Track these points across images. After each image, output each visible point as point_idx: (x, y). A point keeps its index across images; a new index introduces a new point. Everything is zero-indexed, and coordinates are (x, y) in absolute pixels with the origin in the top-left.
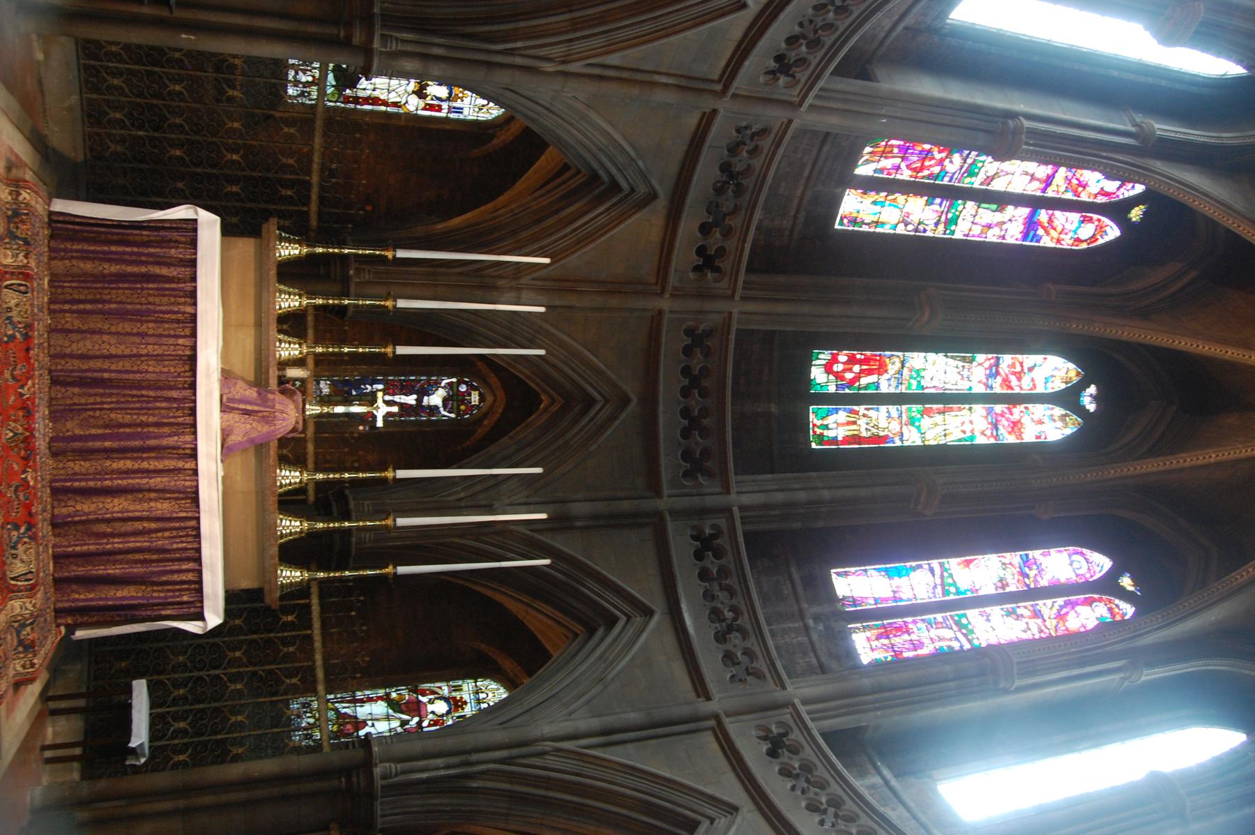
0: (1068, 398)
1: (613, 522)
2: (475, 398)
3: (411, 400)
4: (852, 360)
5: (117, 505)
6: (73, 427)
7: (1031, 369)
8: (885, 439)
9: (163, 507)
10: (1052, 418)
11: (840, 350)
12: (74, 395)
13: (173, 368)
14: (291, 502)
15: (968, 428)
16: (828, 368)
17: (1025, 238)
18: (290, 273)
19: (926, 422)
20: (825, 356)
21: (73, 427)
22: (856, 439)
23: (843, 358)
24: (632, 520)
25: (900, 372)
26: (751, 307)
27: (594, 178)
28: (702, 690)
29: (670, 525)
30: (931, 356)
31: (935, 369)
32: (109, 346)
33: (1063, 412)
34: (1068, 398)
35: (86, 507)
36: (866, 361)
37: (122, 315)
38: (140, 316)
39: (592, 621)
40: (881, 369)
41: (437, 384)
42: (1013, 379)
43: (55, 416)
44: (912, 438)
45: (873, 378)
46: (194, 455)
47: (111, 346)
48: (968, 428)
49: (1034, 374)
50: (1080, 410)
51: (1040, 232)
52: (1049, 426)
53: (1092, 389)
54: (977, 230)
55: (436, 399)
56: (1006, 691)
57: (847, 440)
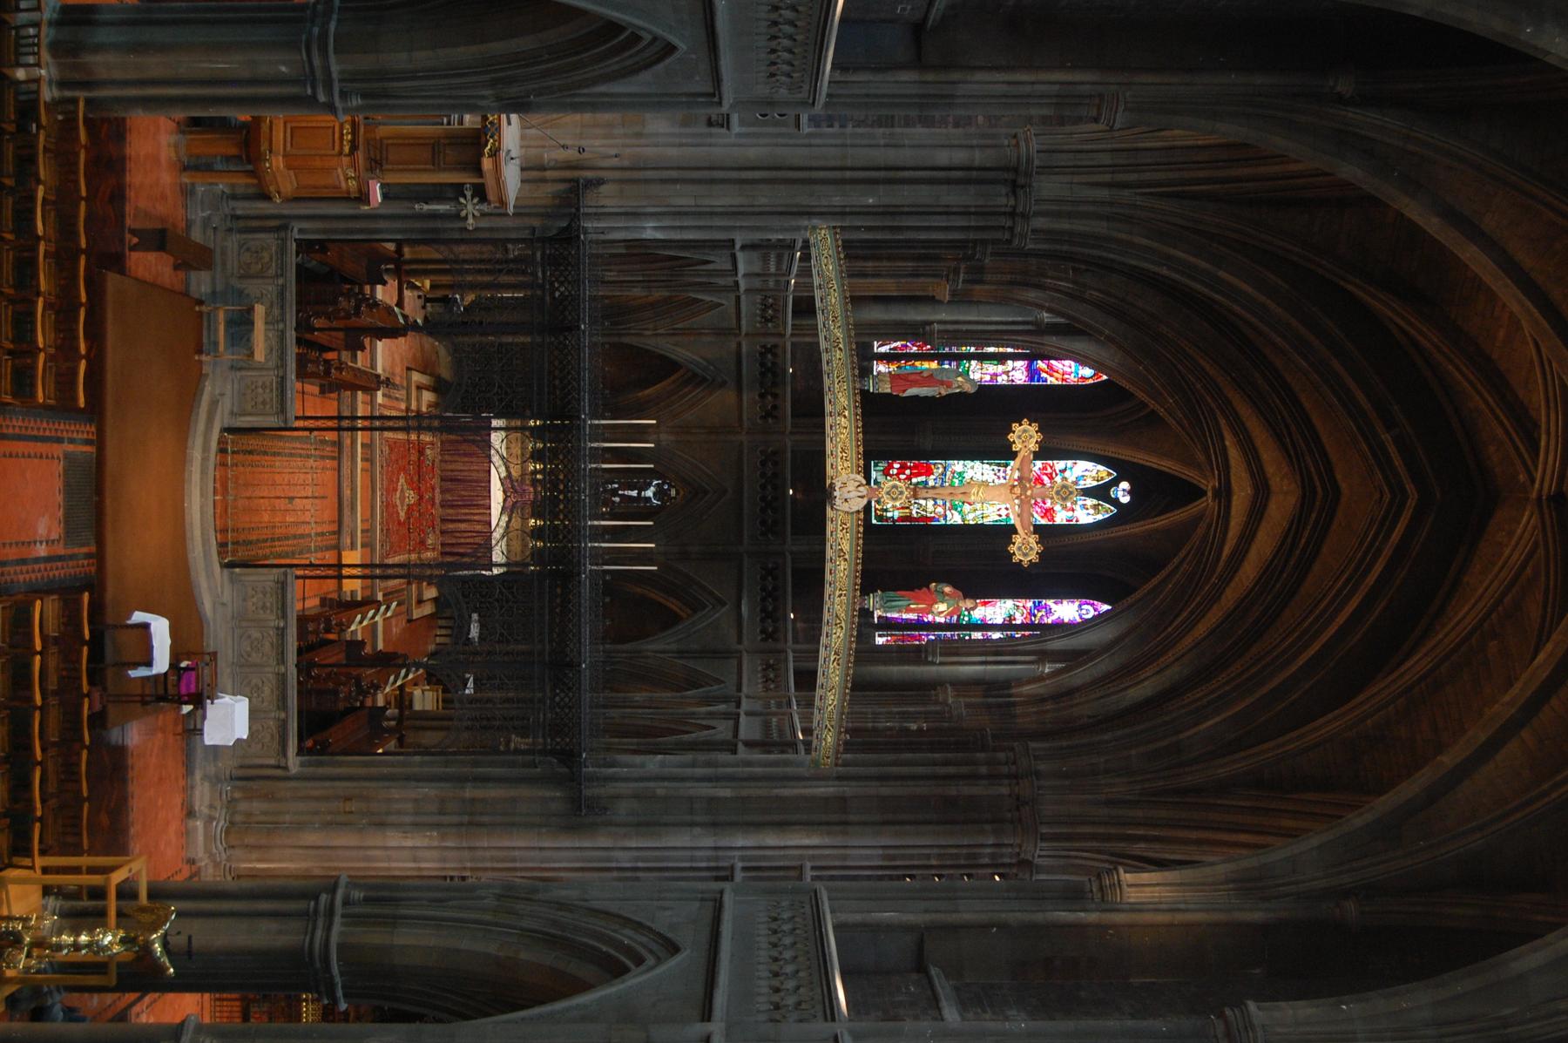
0: (1100, 493)
2: (673, 493)
3: (634, 493)
4: (901, 470)
5: (463, 526)
6: (448, 497)
7: (1063, 471)
8: (932, 519)
9: (478, 528)
10: (1084, 507)
11: (895, 460)
12: (449, 485)
13: (482, 475)
14: (537, 533)
15: (1004, 512)
16: (886, 473)
17: (1032, 379)
18: (536, 433)
19: (967, 508)
20: (883, 465)
21: (448, 497)
22: (909, 518)
23: (897, 466)
25: (944, 474)
26: (798, 437)
27: (695, 375)
28: (740, 641)
30: (969, 463)
31: (978, 471)
32: (460, 466)
33: (1095, 502)
34: (1100, 493)
35: (451, 526)
36: (915, 467)
37: (465, 455)
38: (471, 455)
40: (929, 472)
41: (650, 485)
42: (1046, 479)
43: (442, 492)
44: (955, 519)
45: (923, 478)
46: (489, 508)
47: (460, 466)
48: (1004, 512)
49: (1067, 474)
50: (1115, 502)
51: (1044, 375)
52: (1086, 514)
53: (1125, 485)
54: (988, 378)
55: (649, 493)
56: (933, 663)
57: (901, 519)
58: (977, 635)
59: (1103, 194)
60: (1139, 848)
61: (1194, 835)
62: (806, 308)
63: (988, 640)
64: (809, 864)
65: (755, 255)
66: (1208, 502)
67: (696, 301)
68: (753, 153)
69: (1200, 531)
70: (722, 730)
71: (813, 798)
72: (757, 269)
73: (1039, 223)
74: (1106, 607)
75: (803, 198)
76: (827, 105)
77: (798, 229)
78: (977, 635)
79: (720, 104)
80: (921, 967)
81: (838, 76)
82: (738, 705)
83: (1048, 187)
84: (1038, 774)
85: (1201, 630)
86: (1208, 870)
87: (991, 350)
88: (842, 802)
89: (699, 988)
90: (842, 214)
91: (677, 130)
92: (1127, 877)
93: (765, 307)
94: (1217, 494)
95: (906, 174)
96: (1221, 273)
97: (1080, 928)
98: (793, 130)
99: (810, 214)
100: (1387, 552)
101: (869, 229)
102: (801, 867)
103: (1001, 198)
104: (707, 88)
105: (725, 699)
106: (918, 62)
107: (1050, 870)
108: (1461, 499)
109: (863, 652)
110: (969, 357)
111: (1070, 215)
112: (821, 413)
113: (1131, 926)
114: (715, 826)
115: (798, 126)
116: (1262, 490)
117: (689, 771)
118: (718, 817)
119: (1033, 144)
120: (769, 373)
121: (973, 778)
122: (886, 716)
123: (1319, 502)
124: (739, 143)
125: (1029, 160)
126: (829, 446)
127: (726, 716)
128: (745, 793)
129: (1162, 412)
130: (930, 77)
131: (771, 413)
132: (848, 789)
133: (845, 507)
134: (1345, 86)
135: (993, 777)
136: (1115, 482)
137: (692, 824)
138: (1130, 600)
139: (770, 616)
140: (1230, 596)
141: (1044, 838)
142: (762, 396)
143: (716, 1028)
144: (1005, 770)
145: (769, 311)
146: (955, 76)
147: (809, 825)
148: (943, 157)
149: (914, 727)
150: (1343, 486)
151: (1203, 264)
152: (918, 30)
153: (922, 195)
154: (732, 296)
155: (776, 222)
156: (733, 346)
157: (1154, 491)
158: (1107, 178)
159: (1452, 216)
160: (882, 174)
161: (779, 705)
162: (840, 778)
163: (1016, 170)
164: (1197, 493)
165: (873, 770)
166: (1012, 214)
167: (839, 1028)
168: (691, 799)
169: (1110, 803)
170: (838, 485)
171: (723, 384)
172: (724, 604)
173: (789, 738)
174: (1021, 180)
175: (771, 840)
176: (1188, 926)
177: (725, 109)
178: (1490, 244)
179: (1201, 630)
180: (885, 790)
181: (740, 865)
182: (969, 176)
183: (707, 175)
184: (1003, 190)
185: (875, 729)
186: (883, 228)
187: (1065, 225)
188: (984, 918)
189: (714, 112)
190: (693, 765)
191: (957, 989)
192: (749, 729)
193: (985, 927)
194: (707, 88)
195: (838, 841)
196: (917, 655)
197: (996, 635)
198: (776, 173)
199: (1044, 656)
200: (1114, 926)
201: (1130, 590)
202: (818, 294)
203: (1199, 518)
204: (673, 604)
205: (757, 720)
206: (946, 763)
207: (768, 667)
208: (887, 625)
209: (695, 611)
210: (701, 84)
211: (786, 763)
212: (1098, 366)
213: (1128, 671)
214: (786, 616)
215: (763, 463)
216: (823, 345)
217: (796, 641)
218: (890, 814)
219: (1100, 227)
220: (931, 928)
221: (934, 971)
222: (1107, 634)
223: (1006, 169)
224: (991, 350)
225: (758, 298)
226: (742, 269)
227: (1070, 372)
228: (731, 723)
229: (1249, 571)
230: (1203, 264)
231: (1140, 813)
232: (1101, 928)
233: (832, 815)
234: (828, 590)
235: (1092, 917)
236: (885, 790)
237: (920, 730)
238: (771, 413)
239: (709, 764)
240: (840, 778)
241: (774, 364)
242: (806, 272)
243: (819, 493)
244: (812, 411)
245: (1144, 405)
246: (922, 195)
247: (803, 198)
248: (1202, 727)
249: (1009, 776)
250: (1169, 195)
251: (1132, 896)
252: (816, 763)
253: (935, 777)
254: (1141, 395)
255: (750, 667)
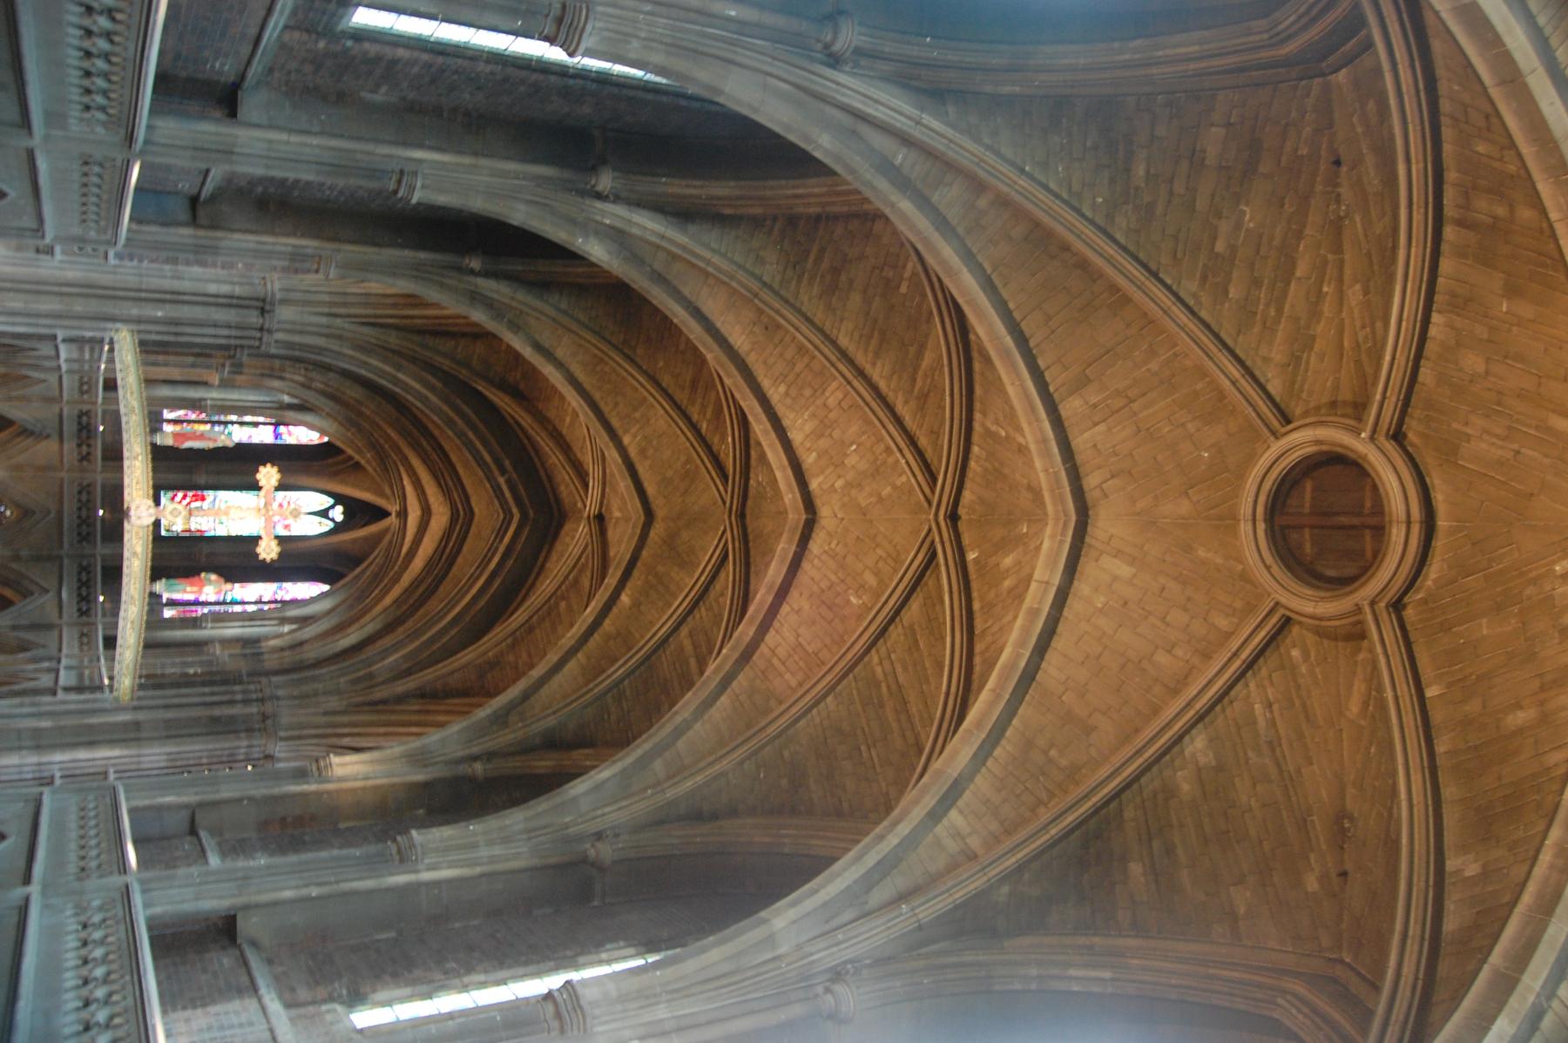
0: (324, 514)
1: (38, 559)
4: (184, 497)
20: (170, 494)
23: (180, 495)
24: (50, 558)
28: (60, 616)
29: (66, 561)
34: (324, 514)
39: (26, 594)
40: (203, 499)
44: (221, 532)
52: (314, 527)
58: (238, 609)
59: (324, 320)
60: (346, 741)
61: (382, 730)
62: (111, 385)
63: (245, 612)
64: (111, 770)
65: (74, 346)
66: (393, 520)
67: (26, 377)
68: (72, 274)
69: (388, 537)
70: (46, 680)
71: (115, 725)
72: (75, 355)
73: (280, 336)
74: (326, 588)
75: (109, 308)
76: (125, 246)
77: (105, 329)
78: (238, 609)
79: (43, 237)
80: (193, 831)
81: (134, 226)
82: (59, 661)
83: (285, 313)
84: (278, 698)
85: (388, 600)
86: (389, 752)
87: (248, 418)
88: (137, 725)
89: (22, 863)
90: (139, 321)
91: (11, 254)
92: (335, 759)
93: (82, 384)
94: (399, 514)
95: (186, 298)
96: (400, 375)
97: (304, 795)
98: (102, 261)
99: (114, 319)
100: (502, 549)
101: (158, 333)
102: (106, 773)
103: (253, 318)
104: (34, 225)
105: (50, 659)
106: (194, 221)
107: (287, 760)
108: (544, 516)
109: (153, 619)
110: (232, 423)
111: (301, 332)
112: (121, 459)
113: (337, 791)
114: (38, 748)
115: (106, 257)
116: (427, 512)
117: (17, 711)
118: (39, 740)
119: (276, 284)
120: (85, 429)
121: (232, 702)
122: (171, 666)
123: (462, 519)
124: (60, 266)
125: (273, 294)
126: (126, 481)
127: (49, 670)
128: (62, 723)
129: (363, 462)
130: (201, 233)
131: (85, 458)
132: (141, 716)
133: (138, 522)
134: (475, 264)
135: (246, 702)
136: (332, 507)
137: (20, 748)
138: (342, 582)
139: (85, 600)
140: (406, 579)
141: (282, 739)
142: (79, 446)
143: (34, 889)
144: (254, 696)
145: (85, 386)
146: (219, 234)
147: (112, 743)
148: (212, 288)
149: (191, 671)
150: (476, 510)
151: (388, 369)
152: (194, 201)
153: (198, 312)
154: (56, 376)
155: (88, 324)
156: (57, 410)
157: (358, 512)
158: (326, 310)
159: (538, 347)
160: (168, 297)
161: (91, 661)
162: (135, 708)
163: (264, 300)
164: (386, 514)
165: (161, 702)
166: (261, 329)
167: (128, 879)
168: (19, 731)
169: (325, 714)
170: (133, 508)
171: (48, 436)
172: (47, 591)
173: (97, 683)
174: (267, 307)
175: (82, 754)
176: (376, 788)
177: (48, 240)
178: (559, 365)
179: (388, 600)
180: (170, 714)
181: (58, 774)
182: (232, 302)
183: (36, 288)
184: (255, 313)
185: (163, 675)
186: (169, 333)
187: (297, 339)
188: (236, 794)
189: (40, 243)
190: (21, 705)
191: (219, 844)
192: (65, 678)
193: (239, 800)
194: (34, 225)
195: (133, 752)
196: (195, 623)
197: (251, 608)
198: (88, 290)
199: (283, 621)
200: (329, 792)
201: (342, 576)
202: (119, 376)
203: (387, 530)
204: (8, 593)
205: (74, 673)
206: (213, 694)
207: (82, 635)
208: (172, 603)
209: (25, 597)
210: (28, 222)
211: (95, 701)
212: (323, 432)
213: (340, 628)
214: (96, 599)
215: (80, 492)
216: (123, 410)
217: (104, 615)
218: (172, 731)
219: (321, 342)
220: (201, 805)
221: (203, 834)
222: (326, 605)
223: (257, 299)
224: (248, 418)
225: (77, 377)
226: (63, 355)
227: (301, 435)
228: (53, 676)
229: (418, 563)
230: (388, 369)
231: (345, 719)
232: (318, 794)
233: (130, 734)
234: (125, 580)
235: (313, 787)
236: (170, 714)
237: (195, 674)
238: (85, 458)
239: (33, 704)
240: (135, 708)
241: (89, 424)
242: (111, 360)
243: (118, 512)
244: (114, 456)
245: (351, 458)
246: (198, 312)
247: (109, 308)
248: (387, 662)
249: (257, 700)
250: (363, 324)
251: (339, 772)
252: (117, 699)
253: (205, 704)
254: (350, 452)
255: (69, 638)
